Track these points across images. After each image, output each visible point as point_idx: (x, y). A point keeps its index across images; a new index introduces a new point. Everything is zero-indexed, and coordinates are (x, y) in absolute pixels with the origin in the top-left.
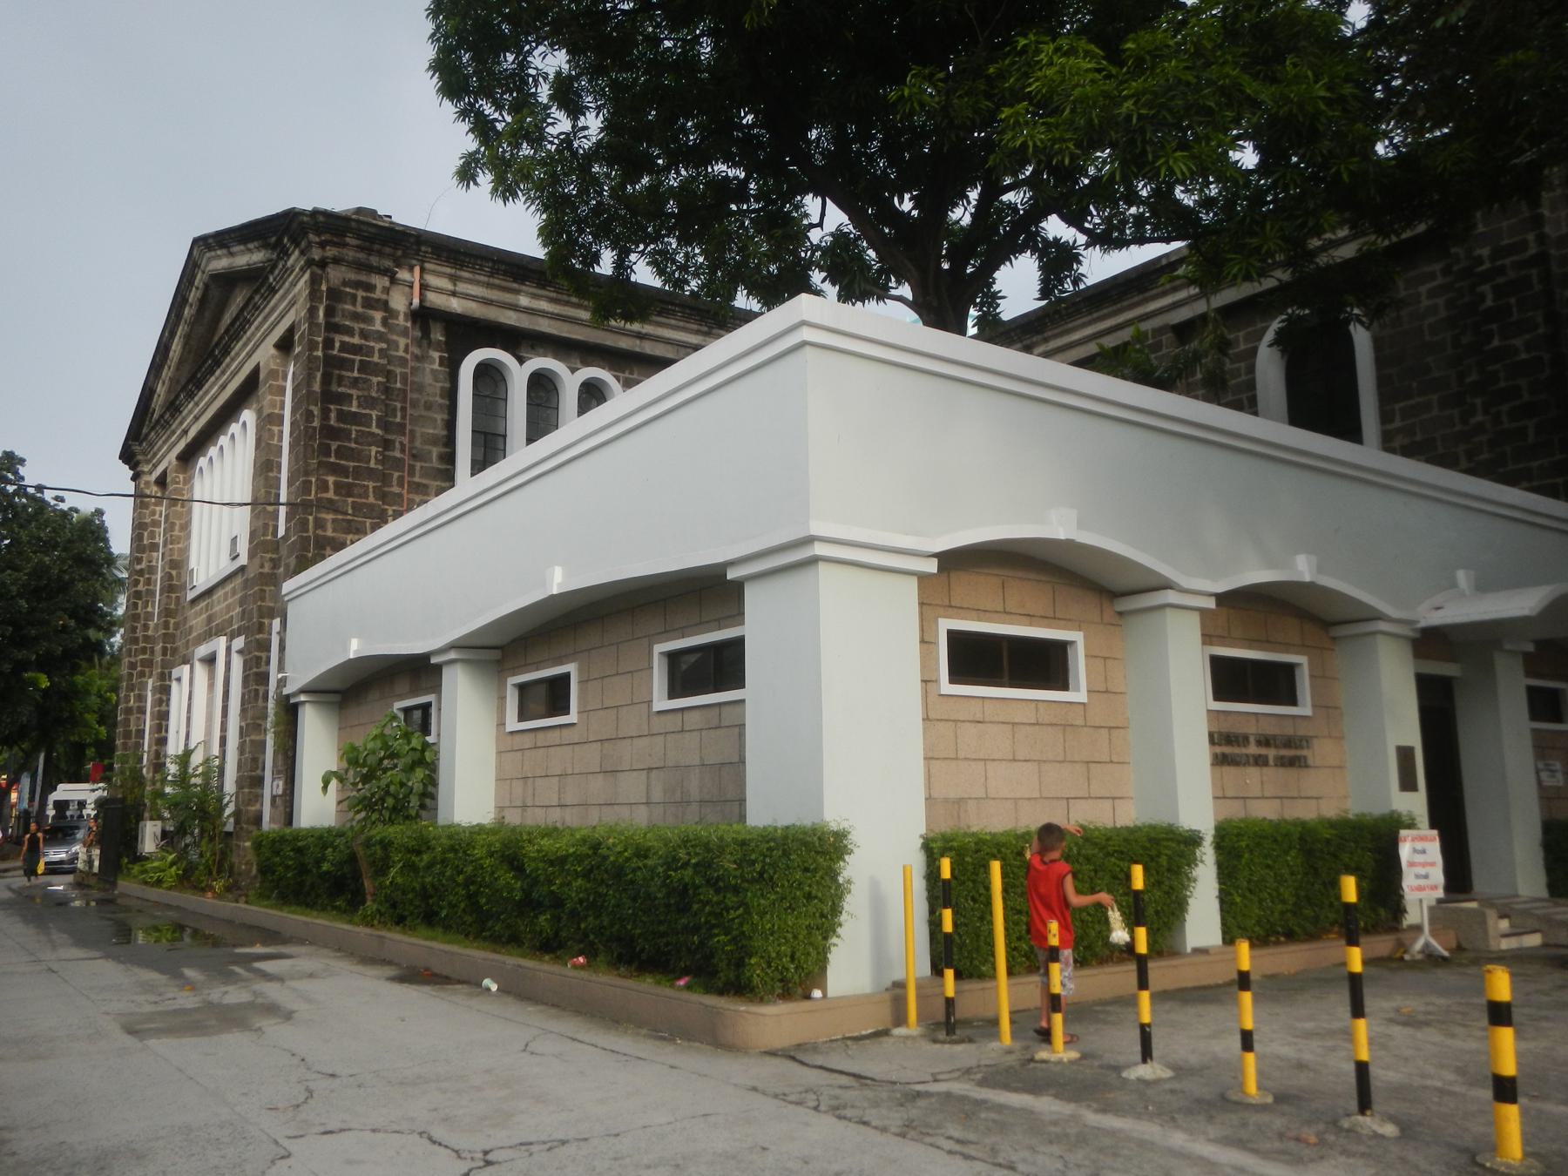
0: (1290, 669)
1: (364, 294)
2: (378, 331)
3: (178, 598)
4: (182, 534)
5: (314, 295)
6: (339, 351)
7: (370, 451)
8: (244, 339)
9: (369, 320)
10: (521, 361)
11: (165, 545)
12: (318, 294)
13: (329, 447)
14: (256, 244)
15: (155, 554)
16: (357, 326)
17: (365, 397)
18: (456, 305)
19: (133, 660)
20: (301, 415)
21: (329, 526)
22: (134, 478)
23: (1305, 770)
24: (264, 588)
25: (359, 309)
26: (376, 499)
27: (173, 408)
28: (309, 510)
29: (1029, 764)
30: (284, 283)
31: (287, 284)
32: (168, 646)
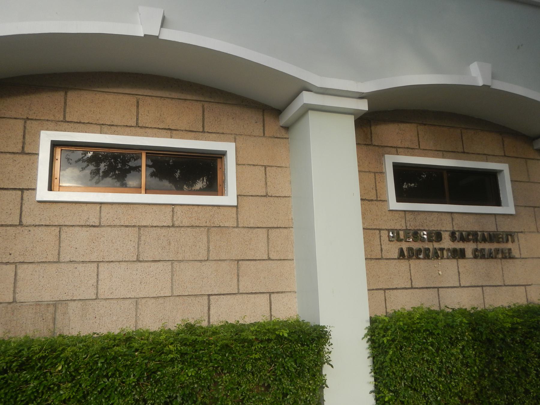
0: (493, 175)
23: (511, 261)
29: (160, 264)
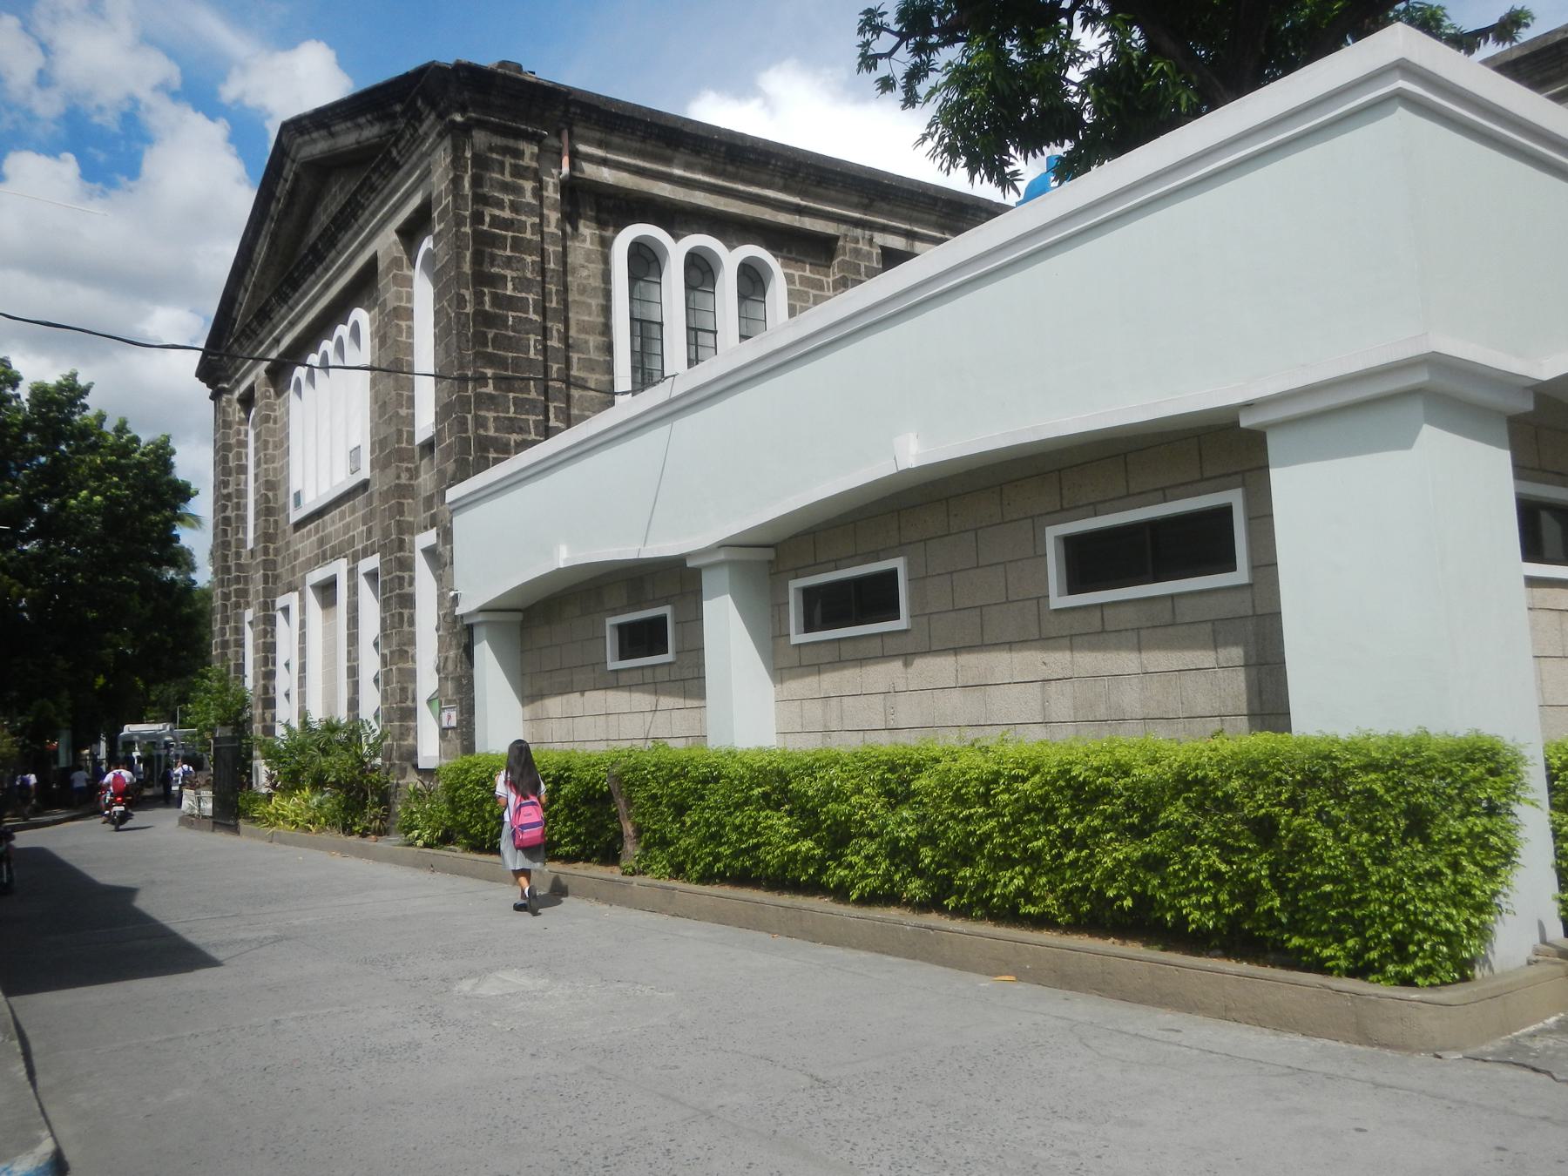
1: (513, 161)
2: (529, 204)
3: (276, 522)
4: (276, 453)
5: (457, 162)
6: (490, 226)
7: (528, 340)
8: (356, 227)
9: (518, 190)
10: (676, 237)
11: (258, 465)
12: (462, 161)
13: (485, 335)
14: (369, 117)
15: (243, 477)
16: (507, 198)
17: (520, 278)
18: (606, 175)
19: (225, 590)
20: (450, 301)
21: (491, 425)
22: (216, 396)
24: (402, 501)
25: (508, 178)
26: (538, 394)
27: (263, 315)
28: (467, 407)
30: (410, 157)
31: (414, 158)
32: (270, 573)
